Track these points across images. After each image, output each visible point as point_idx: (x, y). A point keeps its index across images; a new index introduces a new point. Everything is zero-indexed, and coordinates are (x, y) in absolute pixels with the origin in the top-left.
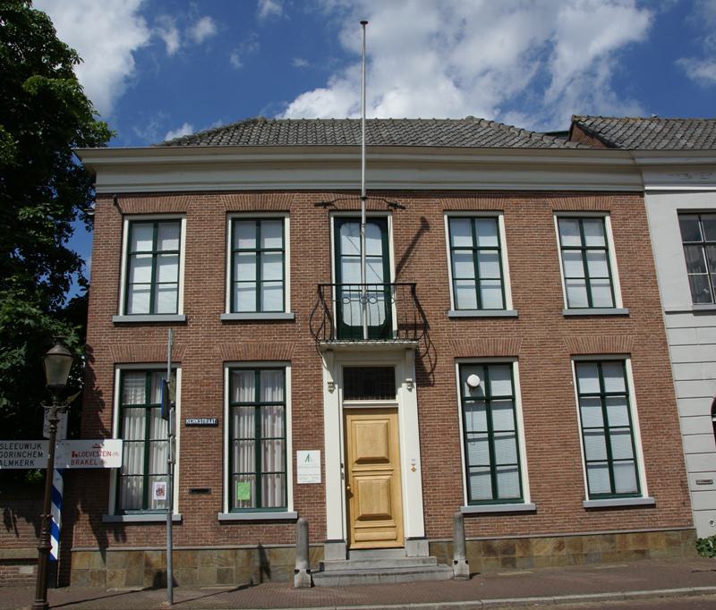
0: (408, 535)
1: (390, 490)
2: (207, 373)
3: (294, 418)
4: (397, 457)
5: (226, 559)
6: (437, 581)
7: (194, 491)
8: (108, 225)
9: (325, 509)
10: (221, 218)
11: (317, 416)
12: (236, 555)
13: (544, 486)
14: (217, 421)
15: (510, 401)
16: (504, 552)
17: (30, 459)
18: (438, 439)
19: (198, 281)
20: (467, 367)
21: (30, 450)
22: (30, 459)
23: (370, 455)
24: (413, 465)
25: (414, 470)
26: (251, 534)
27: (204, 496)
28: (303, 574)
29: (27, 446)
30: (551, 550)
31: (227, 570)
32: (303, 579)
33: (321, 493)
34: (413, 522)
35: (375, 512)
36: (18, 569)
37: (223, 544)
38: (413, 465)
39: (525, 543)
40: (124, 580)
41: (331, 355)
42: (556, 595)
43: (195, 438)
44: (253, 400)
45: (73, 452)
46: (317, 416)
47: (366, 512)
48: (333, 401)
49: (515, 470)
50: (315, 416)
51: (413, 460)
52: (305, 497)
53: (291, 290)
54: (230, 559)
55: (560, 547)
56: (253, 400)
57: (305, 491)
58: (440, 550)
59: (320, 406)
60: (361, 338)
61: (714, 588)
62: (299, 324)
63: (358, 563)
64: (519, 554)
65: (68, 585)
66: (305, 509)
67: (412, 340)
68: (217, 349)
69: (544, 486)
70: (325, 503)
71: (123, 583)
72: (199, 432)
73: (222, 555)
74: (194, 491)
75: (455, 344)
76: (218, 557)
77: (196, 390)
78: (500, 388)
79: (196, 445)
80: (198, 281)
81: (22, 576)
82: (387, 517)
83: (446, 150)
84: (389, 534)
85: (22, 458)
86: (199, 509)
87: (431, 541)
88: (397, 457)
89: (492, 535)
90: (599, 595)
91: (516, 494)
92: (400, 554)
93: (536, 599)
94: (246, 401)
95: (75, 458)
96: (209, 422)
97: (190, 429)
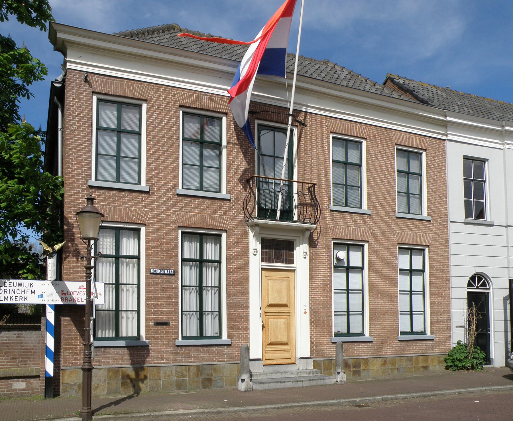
0: (299, 355)
1: (289, 327)
2: (166, 234)
3: (228, 273)
4: (293, 304)
5: (182, 373)
6: (326, 385)
7: (157, 324)
8: (79, 99)
9: (249, 338)
10: (175, 110)
11: (244, 273)
12: (189, 369)
13: (378, 326)
14: (174, 272)
15: (360, 269)
16: (354, 367)
17: (24, 295)
18: (319, 291)
19: (158, 160)
20: (338, 245)
21: (22, 288)
22: (24, 295)
23: (277, 301)
24: (305, 309)
25: (305, 313)
26: (198, 355)
27: (164, 327)
28: (247, 382)
29: (20, 285)
30: (380, 366)
31: (183, 381)
32: (247, 386)
33: (246, 327)
34: (303, 346)
35: (279, 340)
36: (11, 384)
37: (180, 362)
38: (305, 309)
39: (366, 361)
40: (106, 390)
41: (257, 229)
42: (413, 393)
43: (157, 284)
44: (198, 258)
45: (63, 291)
46: (244, 273)
47: (274, 341)
48: (255, 262)
49: (361, 314)
50: (243, 273)
51: (305, 306)
52: (235, 329)
53: (227, 176)
54: (185, 373)
55: (384, 363)
56: (198, 258)
57: (236, 325)
58: (324, 365)
59: (246, 265)
60: (274, 218)
61: (511, 386)
62: (233, 203)
63: (269, 374)
64: (362, 368)
65: (59, 395)
66: (236, 337)
67: (312, 224)
68: (174, 217)
69: (378, 326)
70: (249, 334)
71: (105, 393)
72: (161, 280)
73: (178, 370)
74: (157, 324)
75: (333, 229)
76: (176, 371)
77: (157, 247)
78: (356, 258)
79: (158, 289)
80: (158, 160)
81: (16, 390)
82: (286, 344)
83: (339, 87)
84: (286, 355)
85: (16, 295)
86: (161, 337)
87: (314, 359)
88: (293, 304)
89: (348, 356)
90: (433, 393)
91: (360, 331)
92: (293, 368)
93: (409, 395)
94: (210, 259)
95: (64, 296)
96: (168, 272)
97: (154, 276)
